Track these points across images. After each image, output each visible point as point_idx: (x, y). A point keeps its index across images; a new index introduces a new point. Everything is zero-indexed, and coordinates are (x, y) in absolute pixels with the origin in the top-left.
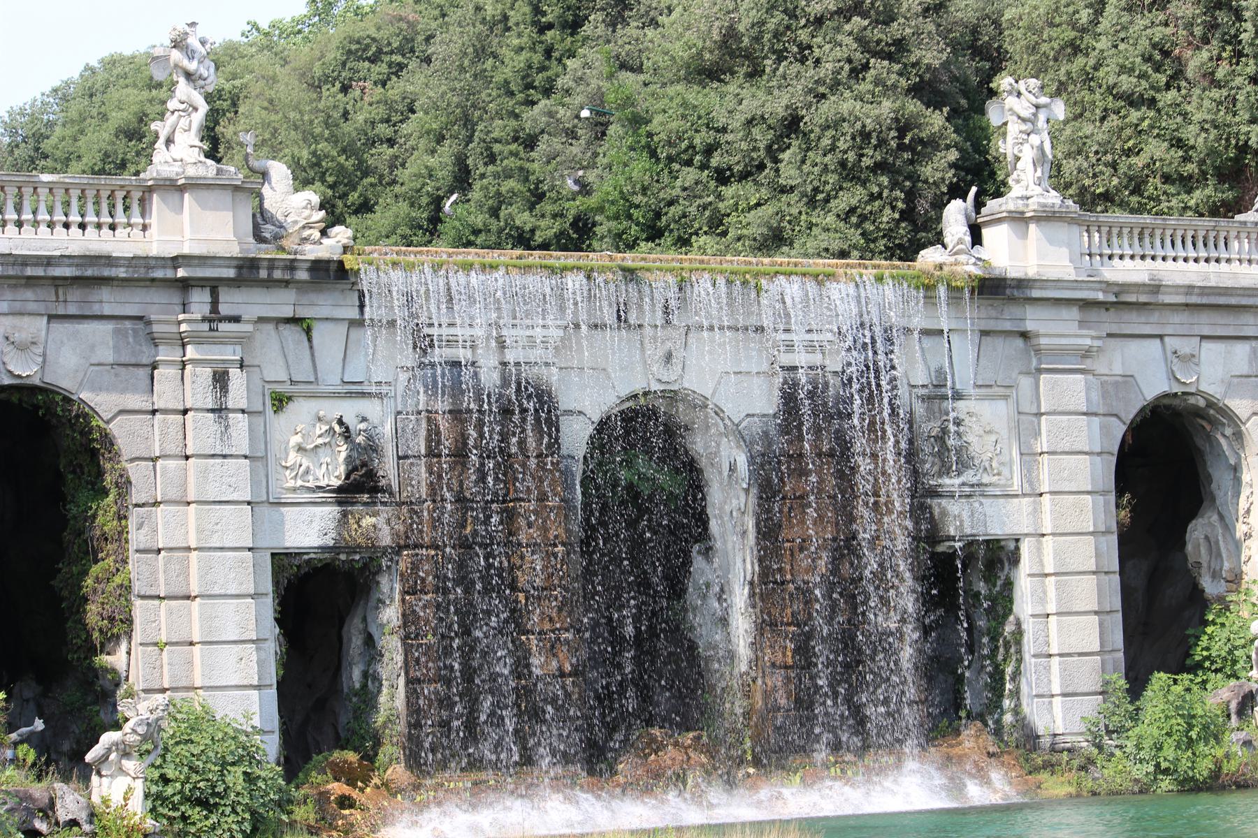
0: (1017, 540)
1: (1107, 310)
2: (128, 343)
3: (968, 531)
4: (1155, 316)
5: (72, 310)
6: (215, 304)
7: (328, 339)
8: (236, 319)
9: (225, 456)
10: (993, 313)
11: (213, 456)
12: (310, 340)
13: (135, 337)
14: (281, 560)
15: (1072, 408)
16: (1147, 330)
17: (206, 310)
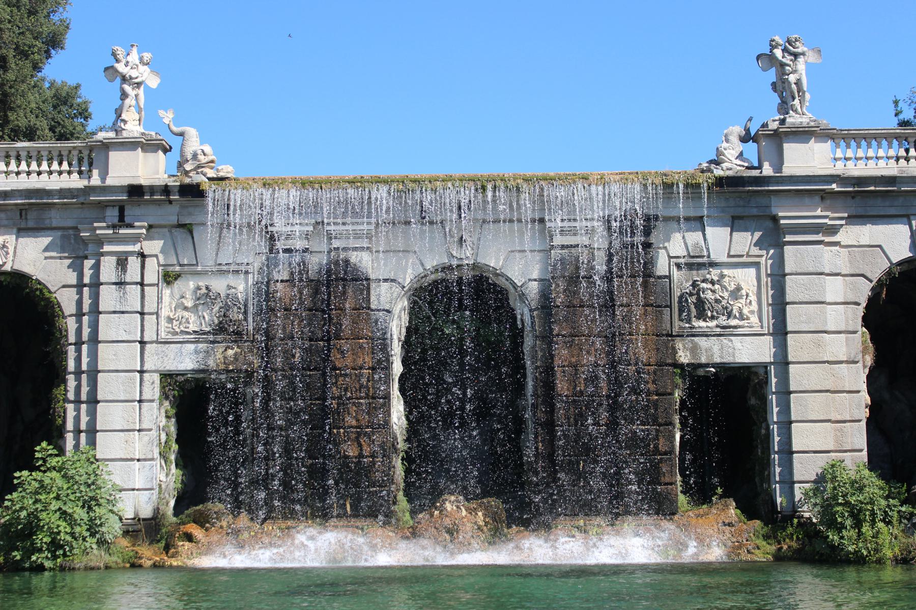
0: (766, 367)
1: (853, 198)
2: (71, 243)
3: (718, 360)
4: (901, 200)
5: (31, 224)
6: (122, 217)
7: (207, 238)
8: (131, 226)
9: (123, 312)
10: (742, 203)
11: (115, 312)
12: (193, 238)
13: (75, 240)
14: (167, 377)
15: (811, 270)
16: (892, 211)
17: (116, 220)
